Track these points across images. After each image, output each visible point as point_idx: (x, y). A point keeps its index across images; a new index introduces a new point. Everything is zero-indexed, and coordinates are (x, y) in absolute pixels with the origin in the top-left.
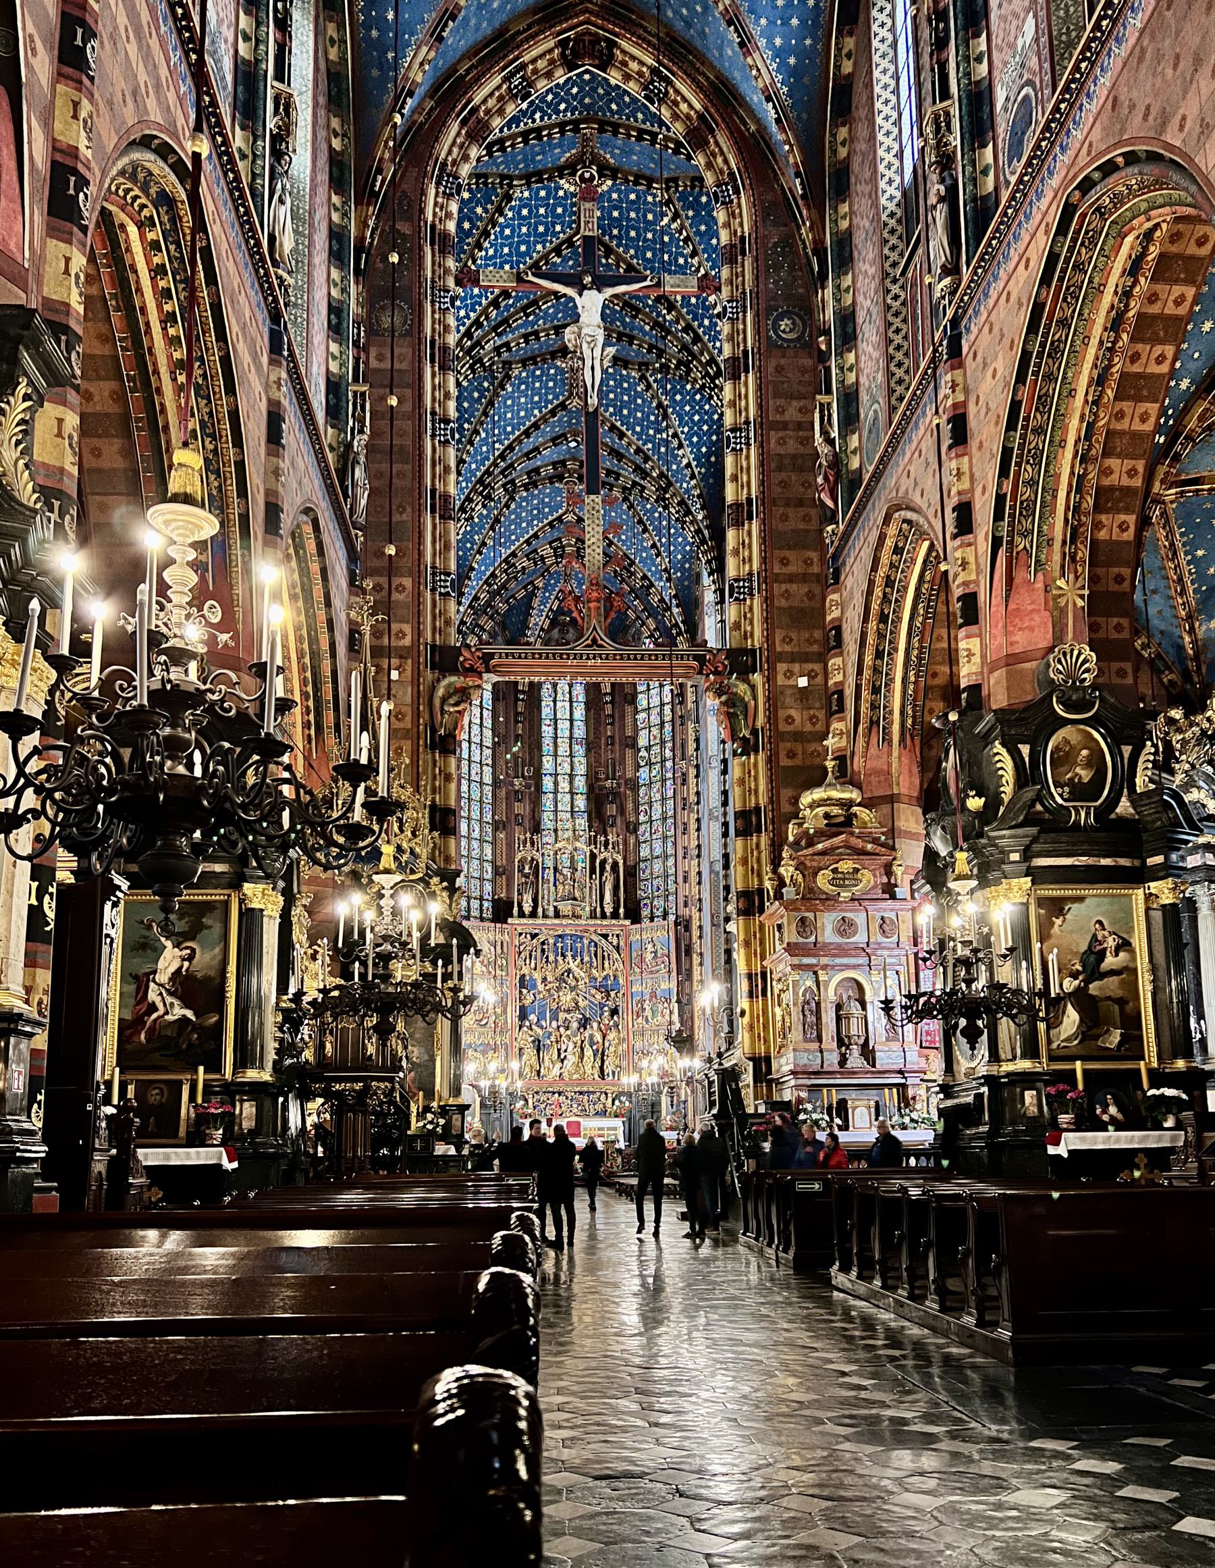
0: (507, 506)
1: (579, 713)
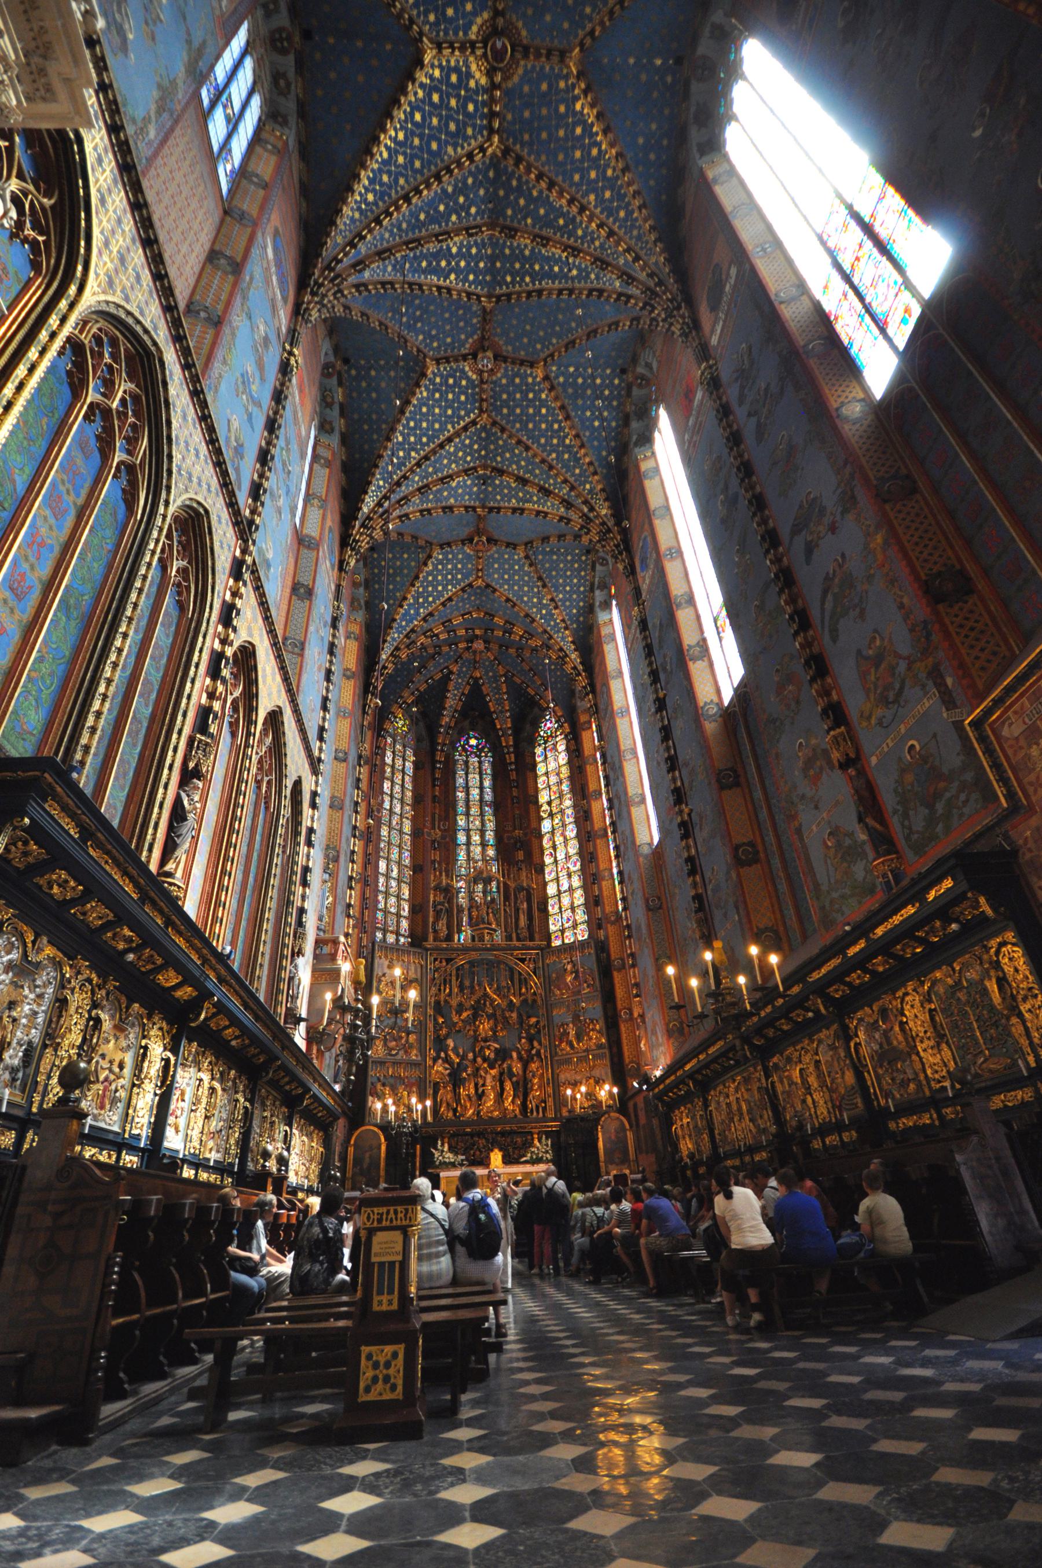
0: (426, 564)
1: (487, 783)
